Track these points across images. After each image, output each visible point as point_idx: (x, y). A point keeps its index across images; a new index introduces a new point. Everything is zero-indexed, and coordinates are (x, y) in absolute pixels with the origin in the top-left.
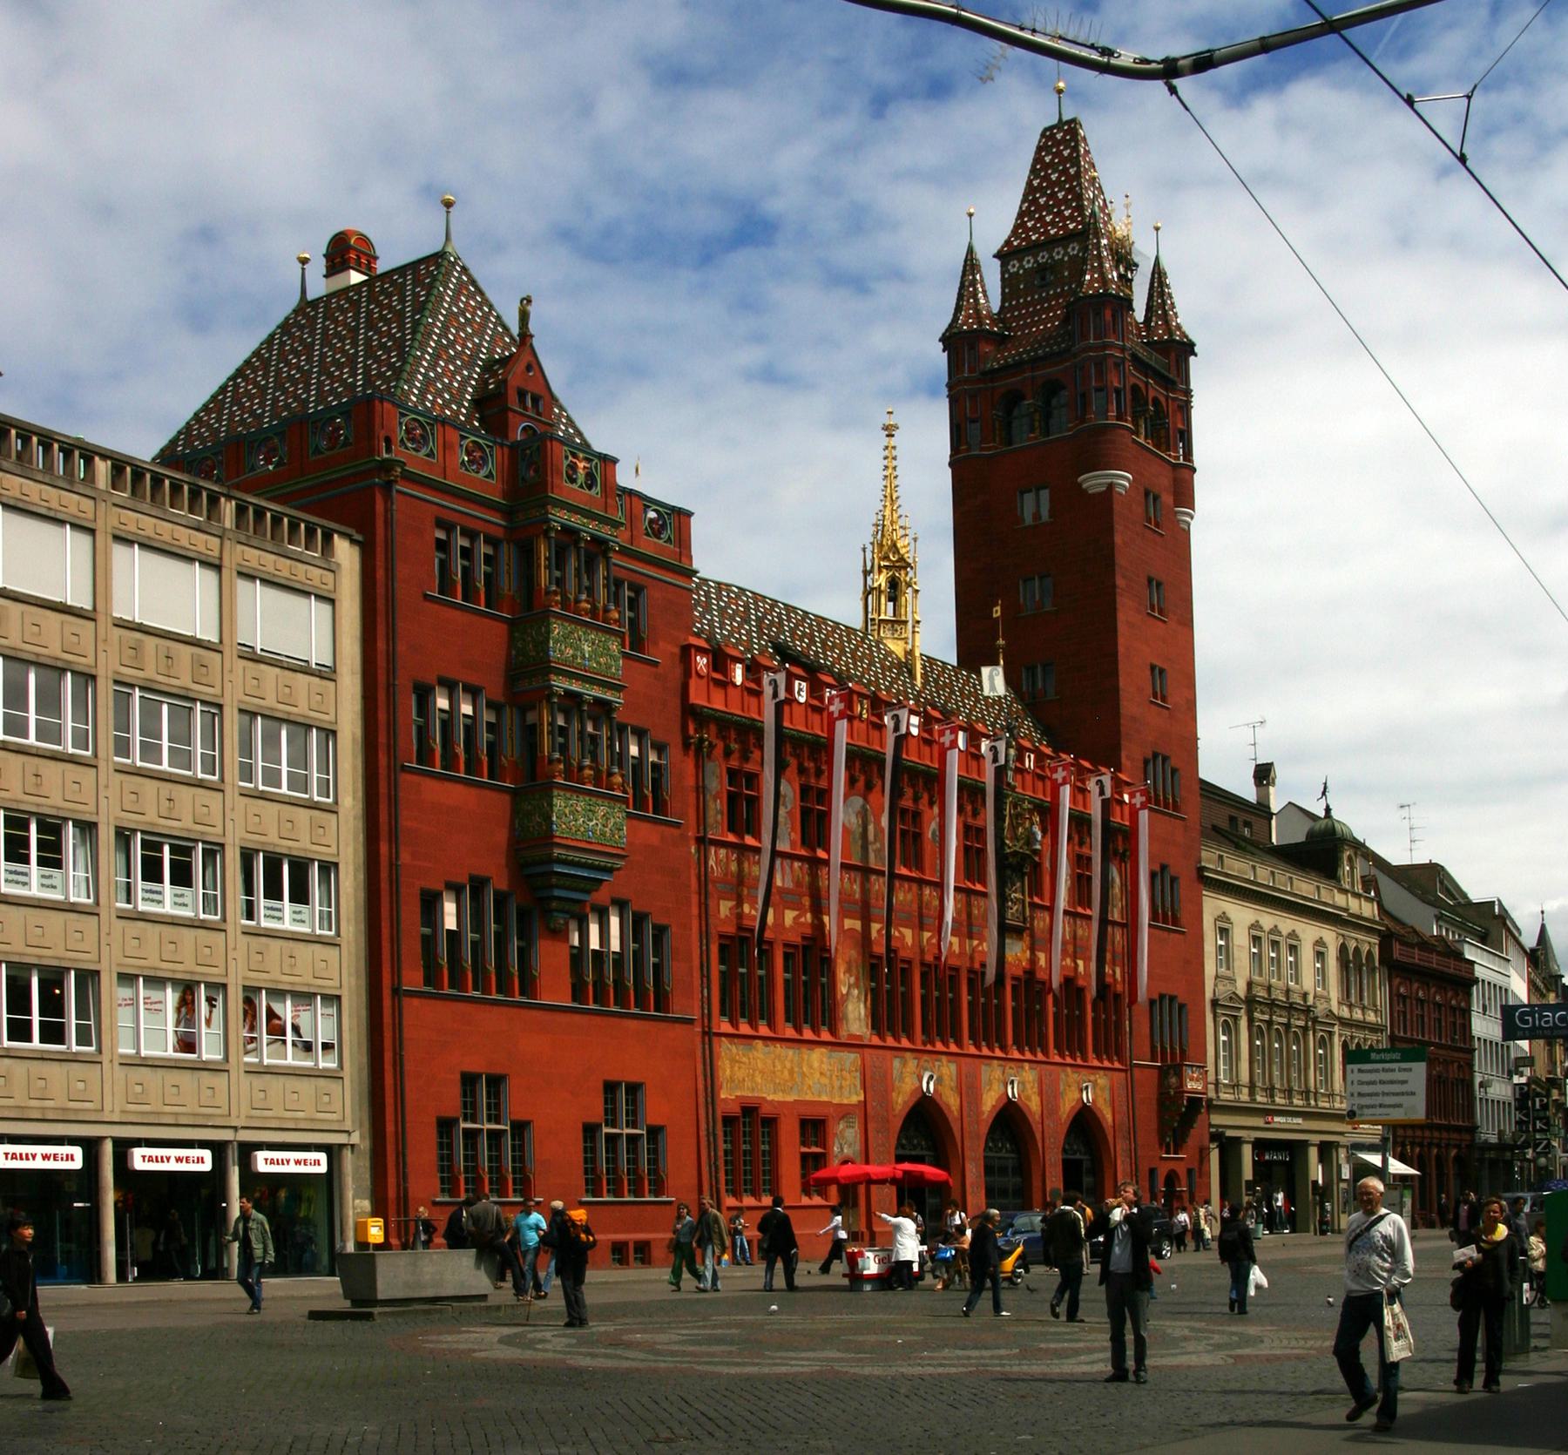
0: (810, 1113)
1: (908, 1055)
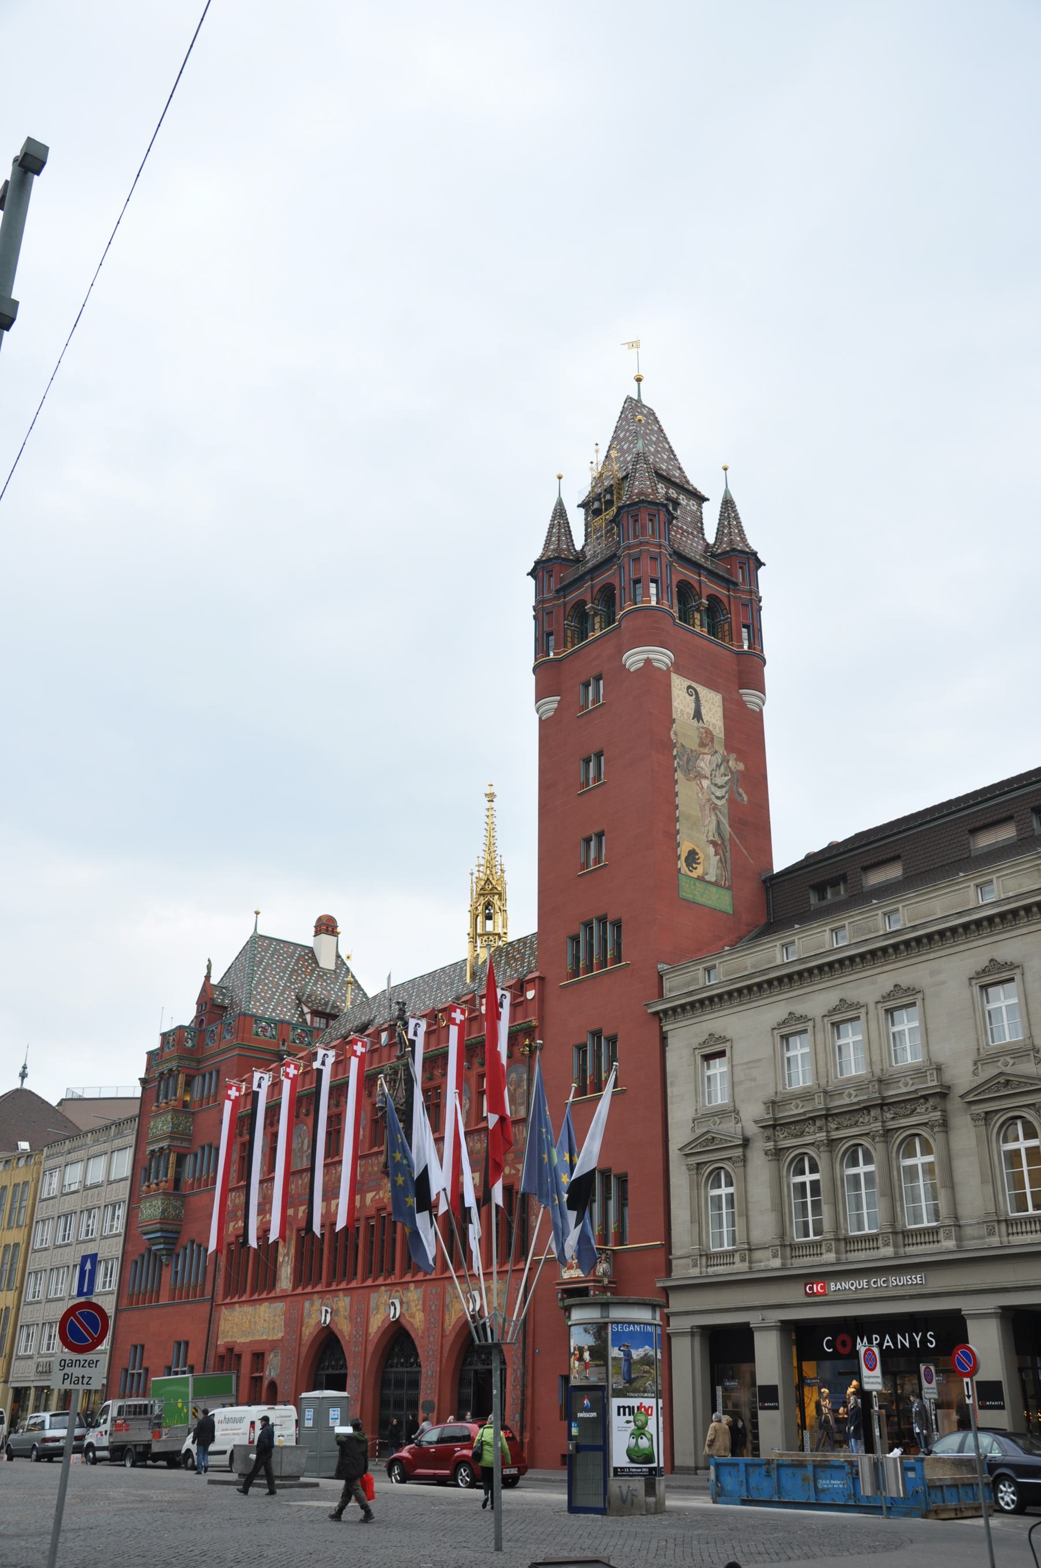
0: (258, 1349)
1: (316, 1296)
